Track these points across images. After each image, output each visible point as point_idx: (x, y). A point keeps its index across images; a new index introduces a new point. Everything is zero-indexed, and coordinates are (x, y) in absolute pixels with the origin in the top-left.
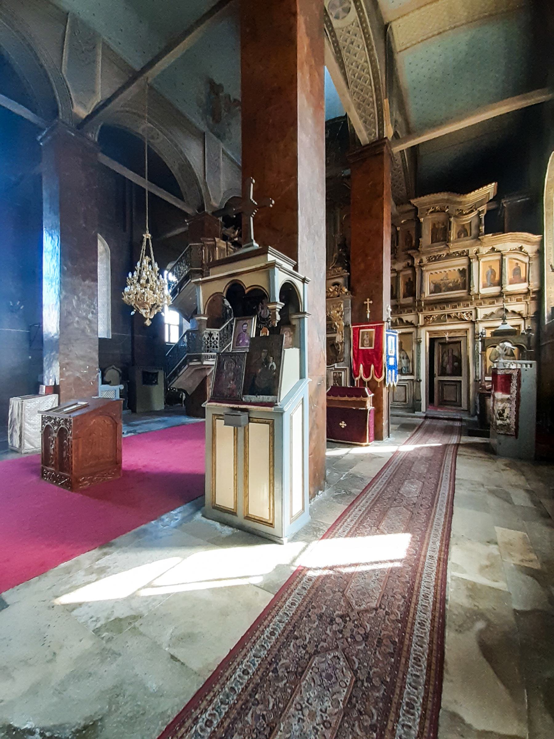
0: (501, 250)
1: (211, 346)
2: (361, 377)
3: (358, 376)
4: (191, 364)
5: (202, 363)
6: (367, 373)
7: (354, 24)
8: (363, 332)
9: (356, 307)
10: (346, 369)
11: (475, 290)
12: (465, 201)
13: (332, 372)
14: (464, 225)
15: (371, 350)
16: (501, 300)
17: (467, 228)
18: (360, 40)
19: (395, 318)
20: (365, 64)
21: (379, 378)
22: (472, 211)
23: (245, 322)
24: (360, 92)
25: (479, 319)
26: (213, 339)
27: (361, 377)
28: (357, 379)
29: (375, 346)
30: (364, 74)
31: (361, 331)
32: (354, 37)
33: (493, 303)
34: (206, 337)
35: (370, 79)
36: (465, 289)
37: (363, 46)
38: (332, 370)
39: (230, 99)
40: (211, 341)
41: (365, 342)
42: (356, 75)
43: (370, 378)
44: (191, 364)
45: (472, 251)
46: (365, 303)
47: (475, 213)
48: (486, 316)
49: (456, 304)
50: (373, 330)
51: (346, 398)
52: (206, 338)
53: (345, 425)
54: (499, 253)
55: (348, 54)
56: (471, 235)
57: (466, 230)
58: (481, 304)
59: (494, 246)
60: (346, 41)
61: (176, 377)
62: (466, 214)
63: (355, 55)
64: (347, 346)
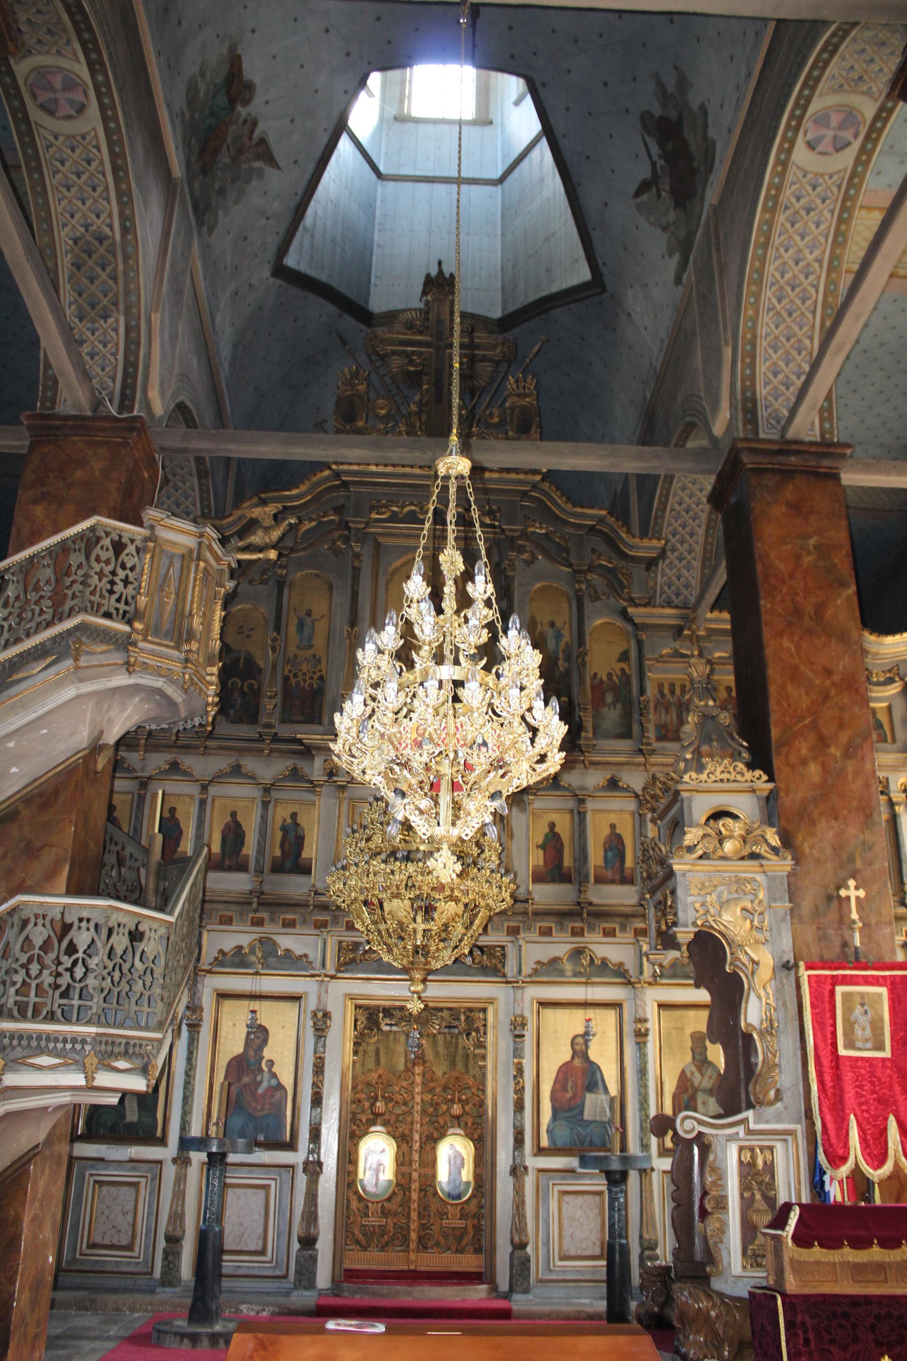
2: (857, 1164)
3: (844, 1159)
7: (835, 177)
8: (847, 996)
9: (806, 907)
10: (792, 1133)
12: (877, 654)
15: (883, 1060)
17: (883, 718)
18: (828, 215)
20: (816, 265)
22: (890, 681)
24: (785, 315)
27: (857, 1164)
28: (845, 1170)
30: (806, 283)
31: (840, 990)
32: (819, 202)
34: (121, 942)
35: (816, 301)
37: (829, 228)
39: (252, 132)
41: (859, 1032)
42: (787, 276)
46: (843, 893)
50: (883, 991)
51: (876, 1253)
52: (119, 952)
55: (788, 225)
56: (894, 741)
57: (879, 725)
60: (798, 199)
62: (878, 684)
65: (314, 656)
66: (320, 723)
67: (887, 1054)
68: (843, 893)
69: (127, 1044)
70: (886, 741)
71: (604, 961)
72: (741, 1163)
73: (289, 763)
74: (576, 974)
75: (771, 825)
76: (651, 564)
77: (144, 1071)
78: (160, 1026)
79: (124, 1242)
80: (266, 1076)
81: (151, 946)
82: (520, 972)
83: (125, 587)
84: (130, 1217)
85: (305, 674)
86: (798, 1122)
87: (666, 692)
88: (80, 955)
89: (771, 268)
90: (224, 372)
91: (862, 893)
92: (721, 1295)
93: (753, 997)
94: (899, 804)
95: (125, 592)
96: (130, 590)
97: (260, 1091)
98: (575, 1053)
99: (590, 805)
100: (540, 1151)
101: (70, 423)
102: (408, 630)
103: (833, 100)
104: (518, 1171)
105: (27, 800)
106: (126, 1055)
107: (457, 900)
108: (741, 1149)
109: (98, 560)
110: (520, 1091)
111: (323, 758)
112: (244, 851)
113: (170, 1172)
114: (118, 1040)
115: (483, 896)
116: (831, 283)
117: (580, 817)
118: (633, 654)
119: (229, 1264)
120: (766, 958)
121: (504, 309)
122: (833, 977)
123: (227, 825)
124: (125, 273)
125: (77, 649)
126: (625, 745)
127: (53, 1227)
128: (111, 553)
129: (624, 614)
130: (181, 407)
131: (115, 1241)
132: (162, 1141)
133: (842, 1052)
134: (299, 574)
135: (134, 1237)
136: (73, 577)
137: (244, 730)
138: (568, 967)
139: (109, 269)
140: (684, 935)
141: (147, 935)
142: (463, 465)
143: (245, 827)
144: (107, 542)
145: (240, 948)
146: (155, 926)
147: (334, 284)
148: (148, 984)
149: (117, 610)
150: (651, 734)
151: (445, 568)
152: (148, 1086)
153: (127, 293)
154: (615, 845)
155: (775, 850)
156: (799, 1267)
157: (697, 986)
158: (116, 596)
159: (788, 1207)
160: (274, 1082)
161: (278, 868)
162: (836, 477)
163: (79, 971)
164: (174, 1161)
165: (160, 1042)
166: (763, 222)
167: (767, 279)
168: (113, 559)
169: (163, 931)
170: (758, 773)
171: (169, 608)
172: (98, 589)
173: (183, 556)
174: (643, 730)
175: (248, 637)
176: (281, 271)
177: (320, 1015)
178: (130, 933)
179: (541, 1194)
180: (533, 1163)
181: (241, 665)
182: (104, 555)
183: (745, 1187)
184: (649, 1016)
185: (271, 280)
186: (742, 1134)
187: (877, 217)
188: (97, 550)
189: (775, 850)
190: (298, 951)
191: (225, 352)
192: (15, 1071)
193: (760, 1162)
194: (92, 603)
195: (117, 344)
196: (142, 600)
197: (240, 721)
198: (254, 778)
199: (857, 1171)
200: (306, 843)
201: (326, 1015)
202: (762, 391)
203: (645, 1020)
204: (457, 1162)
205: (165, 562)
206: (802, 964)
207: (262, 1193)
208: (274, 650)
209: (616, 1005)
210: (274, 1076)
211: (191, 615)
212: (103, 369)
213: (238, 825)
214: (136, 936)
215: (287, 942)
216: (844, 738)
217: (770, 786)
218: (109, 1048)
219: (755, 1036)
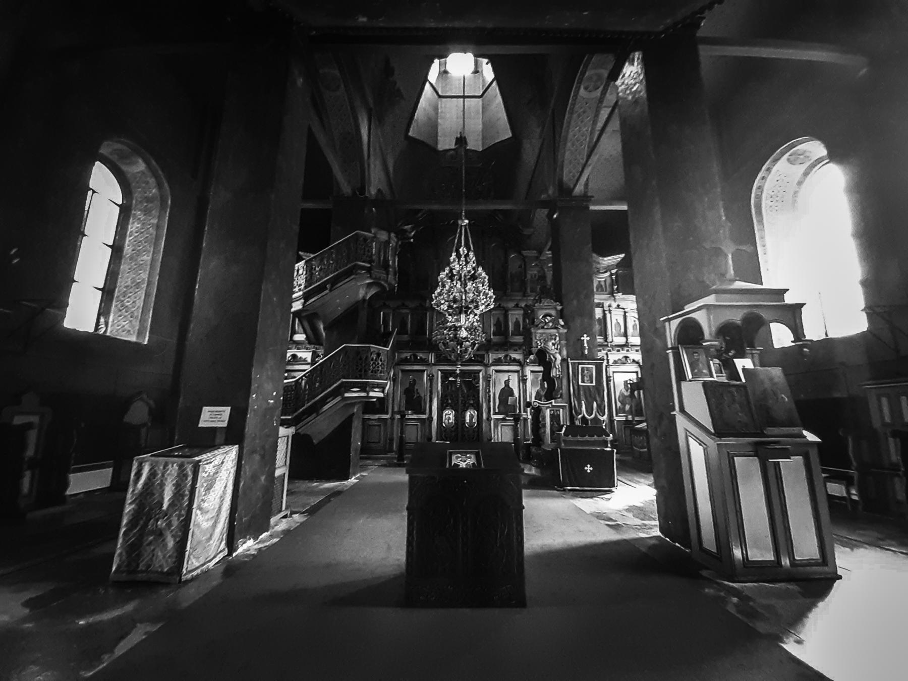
0: (624, 307)
1: (378, 370)
3: (580, 414)
4: (347, 395)
5: (368, 394)
6: (590, 411)
9: (571, 343)
10: (565, 406)
11: (610, 339)
13: (548, 410)
14: (599, 282)
15: (593, 386)
16: (626, 349)
17: (603, 284)
19: (410, 354)
21: (602, 416)
22: (606, 272)
23: (695, 350)
25: (610, 363)
28: (580, 416)
29: (596, 383)
31: (580, 366)
33: (618, 351)
36: (601, 336)
38: (548, 407)
40: (378, 364)
41: (586, 378)
43: (593, 416)
44: (347, 395)
45: (606, 304)
46: (582, 338)
47: (608, 274)
48: (615, 362)
49: (601, 348)
50: (594, 367)
53: (591, 469)
54: (623, 310)
56: (606, 291)
57: (601, 286)
58: (609, 351)
59: (620, 304)
61: (314, 415)
63: (582, 122)
64: (565, 382)
67: (594, 384)
68: (582, 338)
70: (603, 291)
71: (514, 358)
72: (550, 414)
74: (506, 362)
75: (561, 319)
76: (529, 237)
77: (383, 392)
79: (377, 441)
81: (382, 357)
82: (489, 362)
86: (567, 403)
87: (533, 277)
89: (571, 134)
90: (392, 176)
91: (588, 338)
92: (543, 449)
93: (555, 369)
94: (607, 311)
96: (370, 254)
98: (505, 386)
99: (510, 312)
100: (495, 414)
102: (451, 270)
103: (592, 72)
104: (489, 419)
106: (377, 387)
107: (469, 342)
108: (550, 411)
110: (490, 396)
113: (389, 421)
115: (477, 340)
116: (591, 139)
117: (506, 317)
118: (523, 266)
119: (408, 446)
120: (559, 357)
121: (483, 146)
122: (579, 362)
126: (521, 294)
129: (520, 253)
130: (379, 190)
132: (387, 413)
133: (580, 383)
135: (380, 439)
138: (504, 361)
140: (534, 350)
142: (467, 221)
145: (407, 357)
147: (425, 141)
150: (529, 290)
151: (461, 253)
154: (517, 324)
155: (562, 326)
156: (565, 441)
157: (539, 365)
159: (563, 426)
160: (418, 395)
162: (588, 208)
163: (363, 365)
164: (390, 418)
165: (387, 384)
166: (568, 118)
167: (569, 139)
169: (386, 352)
170: (558, 303)
171: (382, 258)
174: (526, 289)
177: (431, 375)
179: (496, 426)
180: (493, 417)
183: (551, 420)
184: (527, 374)
186: (551, 406)
187: (609, 110)
189: (562, 326)
190: (423, 357)
191: (391, 169)
192: (347, 393)
193: (556, 414)
196: (374, 257)
199: (584, 416)
201: (433, 376)
202: (565, 179)
203: (526, 376)
204: (472, 417)
206: (569, 359)
207: (416, 426)
209: (517, 371)
210: (418, 393)
214: (379, 355)
215: (420, 355)
216: (585, 292)
217: (561, 307)
219: (555, 379)
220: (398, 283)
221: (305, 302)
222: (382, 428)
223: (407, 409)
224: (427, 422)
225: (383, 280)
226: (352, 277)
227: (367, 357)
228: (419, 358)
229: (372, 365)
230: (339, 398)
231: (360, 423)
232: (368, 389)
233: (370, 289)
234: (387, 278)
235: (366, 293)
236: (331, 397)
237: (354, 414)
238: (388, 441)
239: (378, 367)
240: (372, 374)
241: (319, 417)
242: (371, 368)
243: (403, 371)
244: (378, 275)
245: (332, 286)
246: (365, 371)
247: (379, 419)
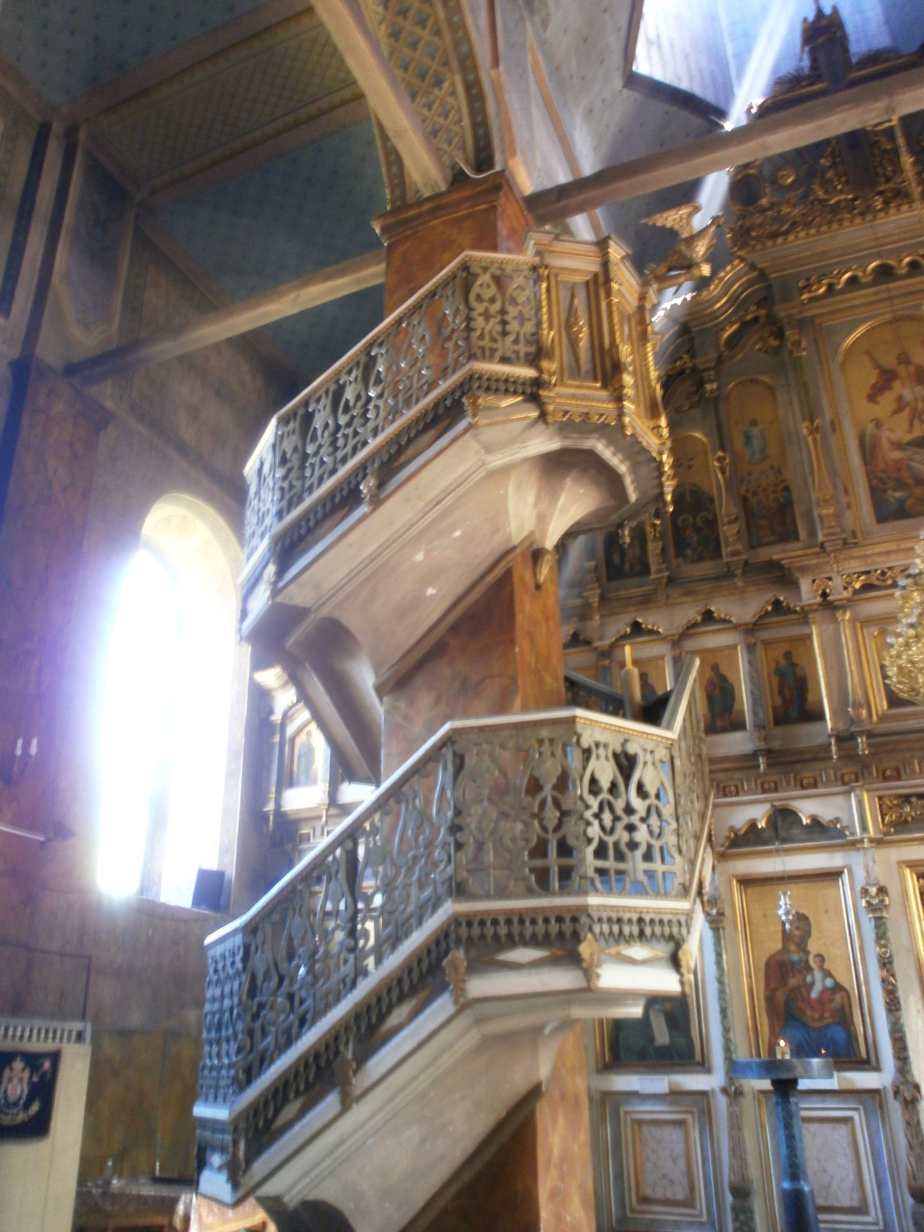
1: (633, 845)
5: (589, 974)
26: (641, 791)
34: (605, 771)
40: (629, 810)
52: (605, 784)
61: (331, 1102)
65: (772, 468)
66: (797, 538)
69: (640, 921)
73: (769, 596)
77: (675, 962)
78: (685, 890)
80: (818, 975)
83: (522, 324)
84: (682, 1163)
85: (765, 490)
88: (548, 791)
95: (522, 332)
97: (814, 995)
101: (426, 207)
105: (455, 629)
109: (479, 298)
111: (811, 578)
112: (736, 707)
113: (721, 1103)
114: (626, 916)
123: (711, 683)
124: (449, 21)
125: (474, 405)
127: (584, 1202)
128: (493, 290)
131: (669, 1195)
132: (704, 1066)
134: (732, 385)
135: (692, 1188)
136: (452, 326)
137: (706, 568)
139: (429, 24)
141: (641, 760)
143: (731, 678)
144: (485, 278)
146: (650, 746)
148: (656, 830)
149: (517, 353)
152: (682, 983)
153: (457, 44)
158: (511, 338)
160: (829, 982)
161: (781, 719)
163: (551, 815)
164: (725, 1091)
165: (689, 915)
168: (498, 297)
169: (662, 753)
172: (487, 331)
173: (587, 284)
175: (690, 467)
176: (633, 80)
177: (873, 890)
178: (616, 756)
181: (688, 499)
182: (487, 294)
185: (626, 92)
188: (475, 289)
194: (483, 349)
195: (459, 109)
197: (701, 559)
198: (730, 622)
200: (810, 685)
201: (882, 890)
205: (564, 294)
208: (723, 471)
210: (828, 974)
211: (613, 344)
212: (450, 143)
213: (723, 679)
218: (616, 928)
220: (672, 451)
221: (280, 574)
222: (695, 1134)
223: (802, 1050)
224: (895, 1109)
225: (603, 430)
226: (463, 424)
227: (563, 783)
228: (805, 821)
229: (597, 816)
230: (442, 1007)
231: (584, 1136)
232: (584, 949)
233: (555, 497)
234: (621, 414)
235: (542, 520)
236: (402, 999)
237: (534, 1093)
238: (729, 1199)
239: (631, 828)
240: (600, 863)
241: (359, 1112)
242: (594, 831)
243: (746, 882)
244: (577, 408)
245: (381, 485)
246: (565, 850)
247: (676, 1095)
